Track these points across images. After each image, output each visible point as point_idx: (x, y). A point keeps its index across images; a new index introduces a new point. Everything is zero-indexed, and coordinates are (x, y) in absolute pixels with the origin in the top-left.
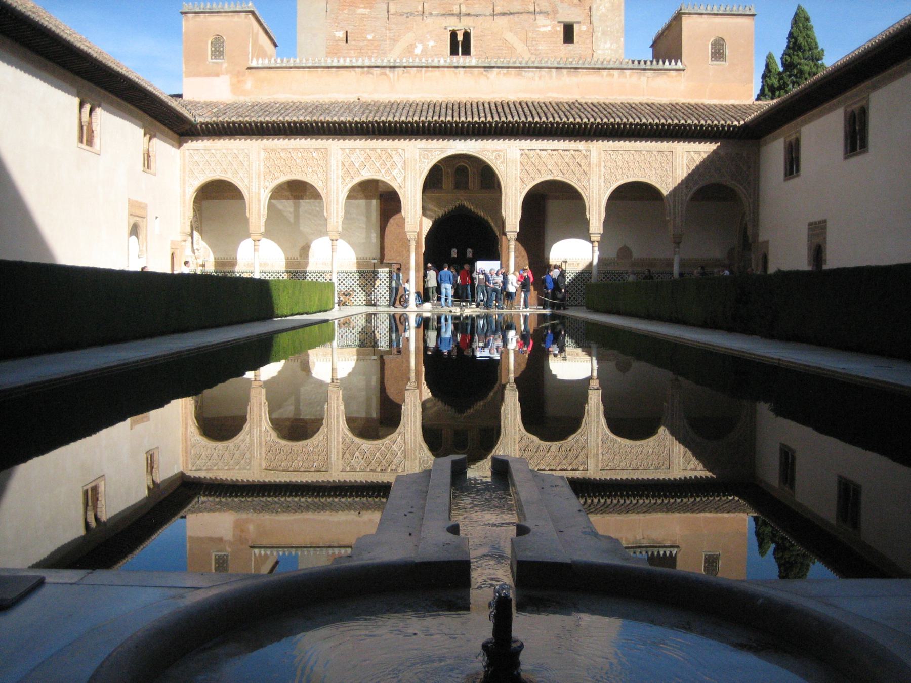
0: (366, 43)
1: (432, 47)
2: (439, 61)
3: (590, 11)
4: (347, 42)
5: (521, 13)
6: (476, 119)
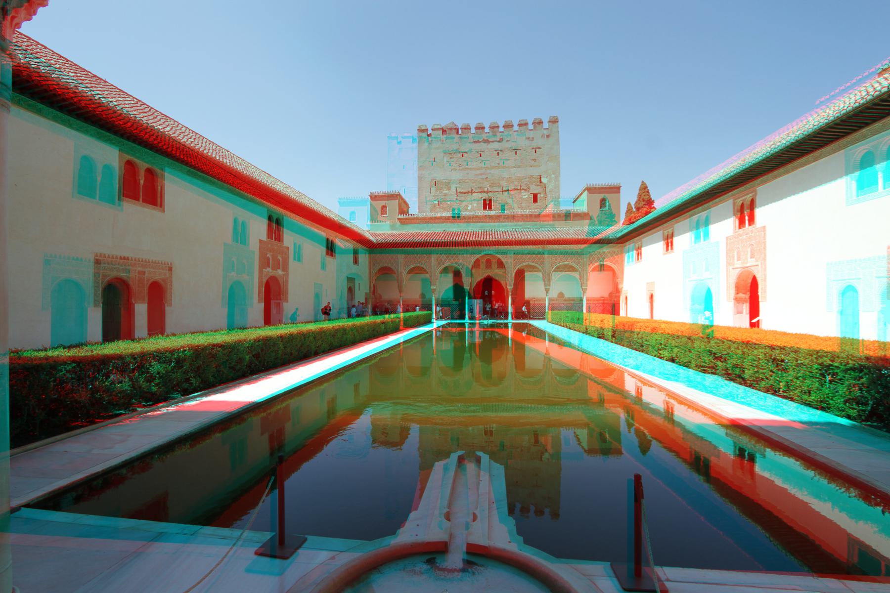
3: (545, 188)
6: (494, 239)
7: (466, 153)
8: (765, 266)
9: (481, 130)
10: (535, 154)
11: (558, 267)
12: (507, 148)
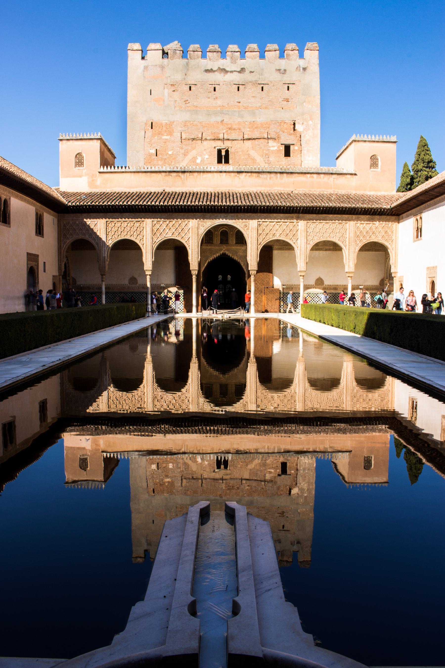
0: (168, 156)
1: (207, 158)
2: (211, 168)
4: (156, 156)
5: (260, 138)
6: (232, 204)
10: (288, 91)
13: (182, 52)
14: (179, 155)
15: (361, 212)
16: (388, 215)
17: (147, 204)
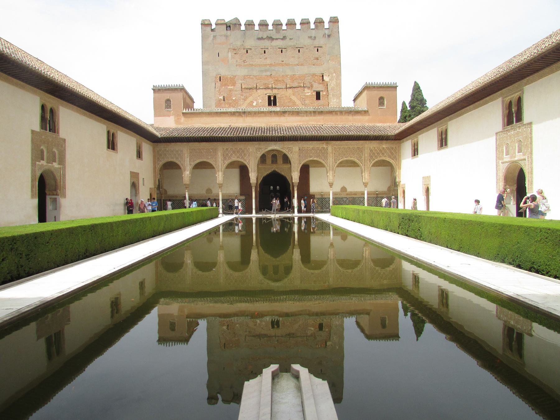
1: (260, 102)
2: (263, 109)
3: (327, 85)
4: (224, 101)
5: (298, 87)
7: (251, 49)
8: (532, 160)
9: (264, 27)
10: (317, 53)
11: (341, 163)
12: (290, 46)
13: (240, 25)
14: (240, 100)
15: (372, 139)
16: (392, 140)
17: (218, 135)
